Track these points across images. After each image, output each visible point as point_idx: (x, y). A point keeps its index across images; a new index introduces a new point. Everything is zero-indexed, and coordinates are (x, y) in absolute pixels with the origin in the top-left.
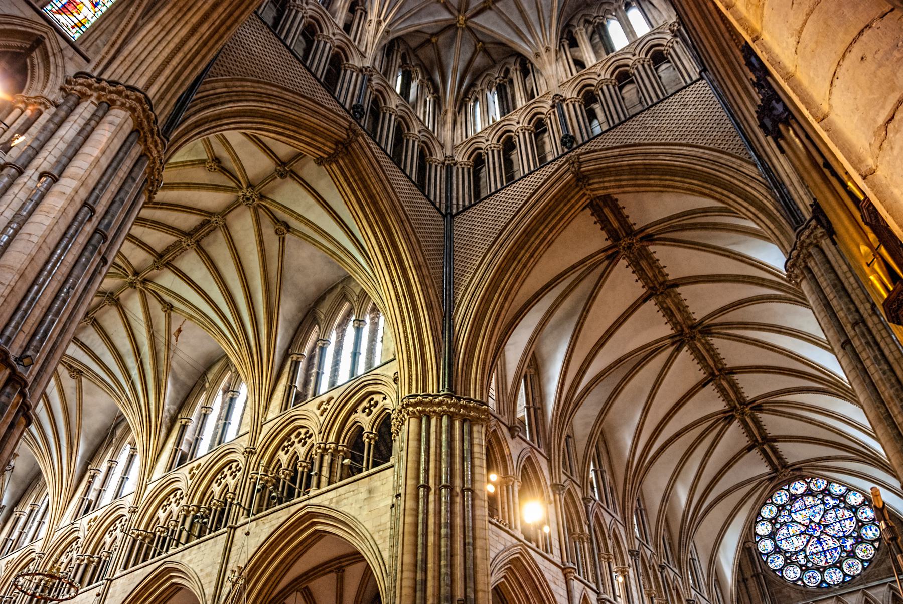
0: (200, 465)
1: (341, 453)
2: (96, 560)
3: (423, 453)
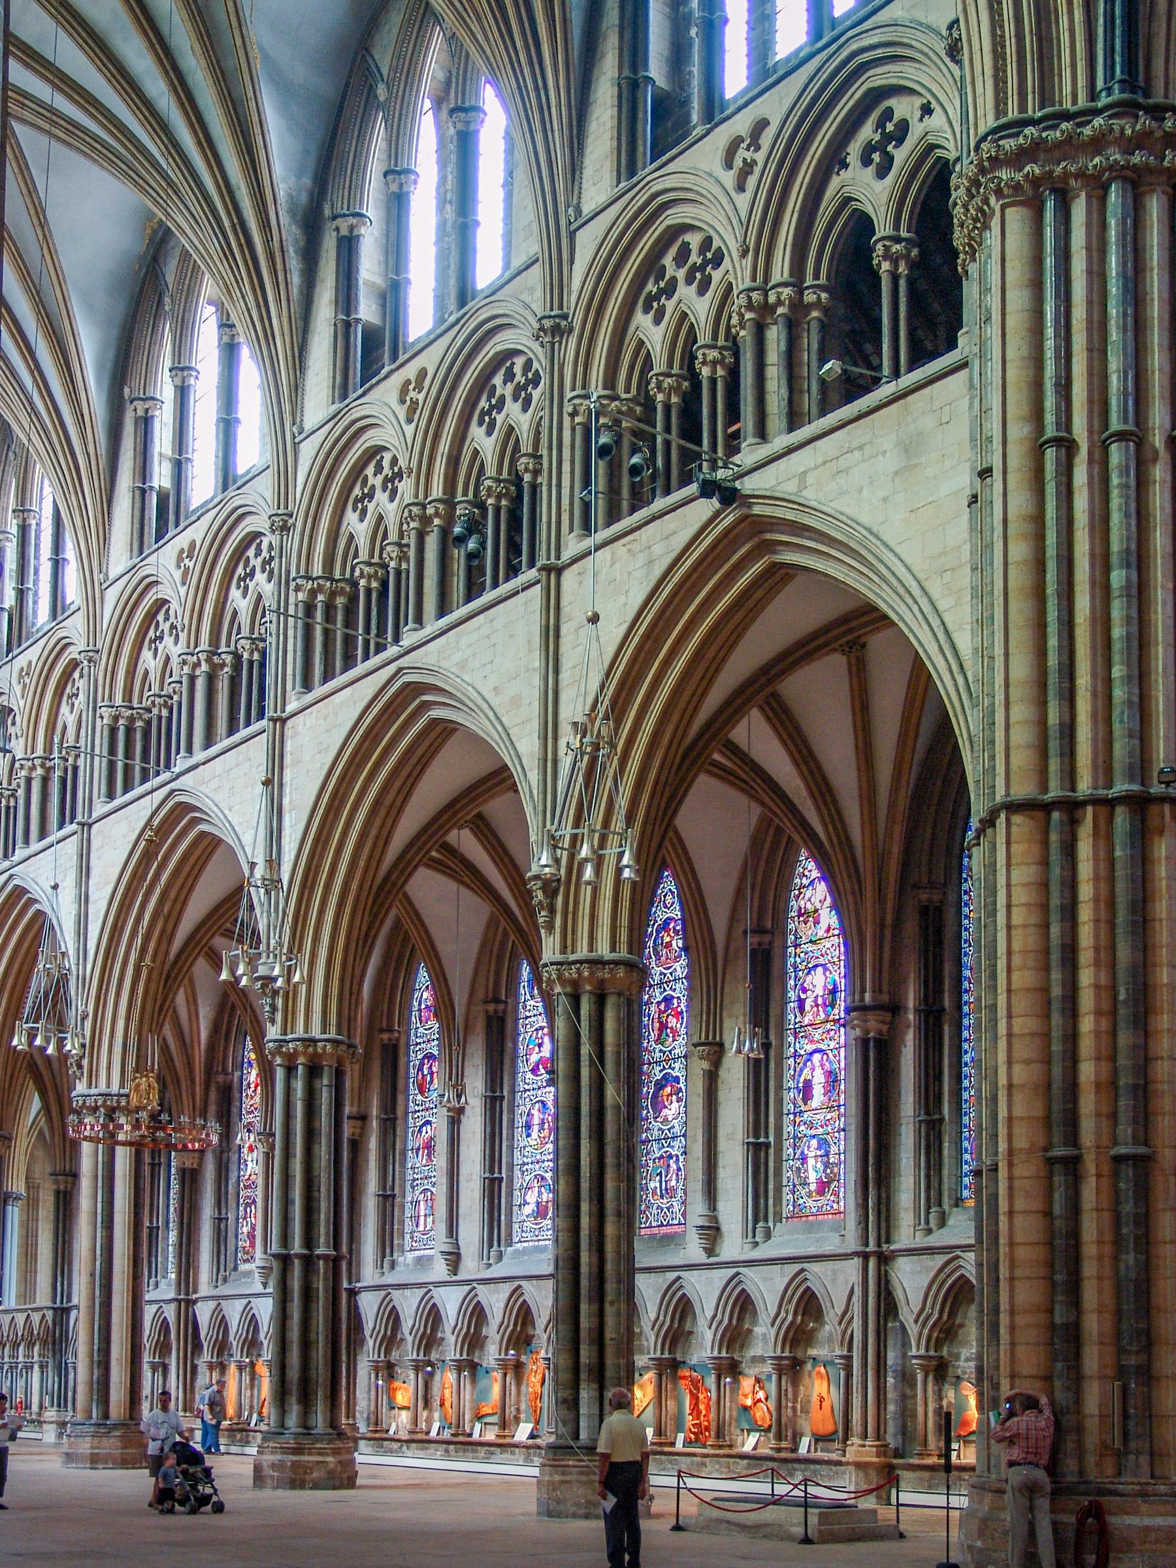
0: (423, 373)
1: (815, 314)
2: (228, 659)
3: (1050, 332)
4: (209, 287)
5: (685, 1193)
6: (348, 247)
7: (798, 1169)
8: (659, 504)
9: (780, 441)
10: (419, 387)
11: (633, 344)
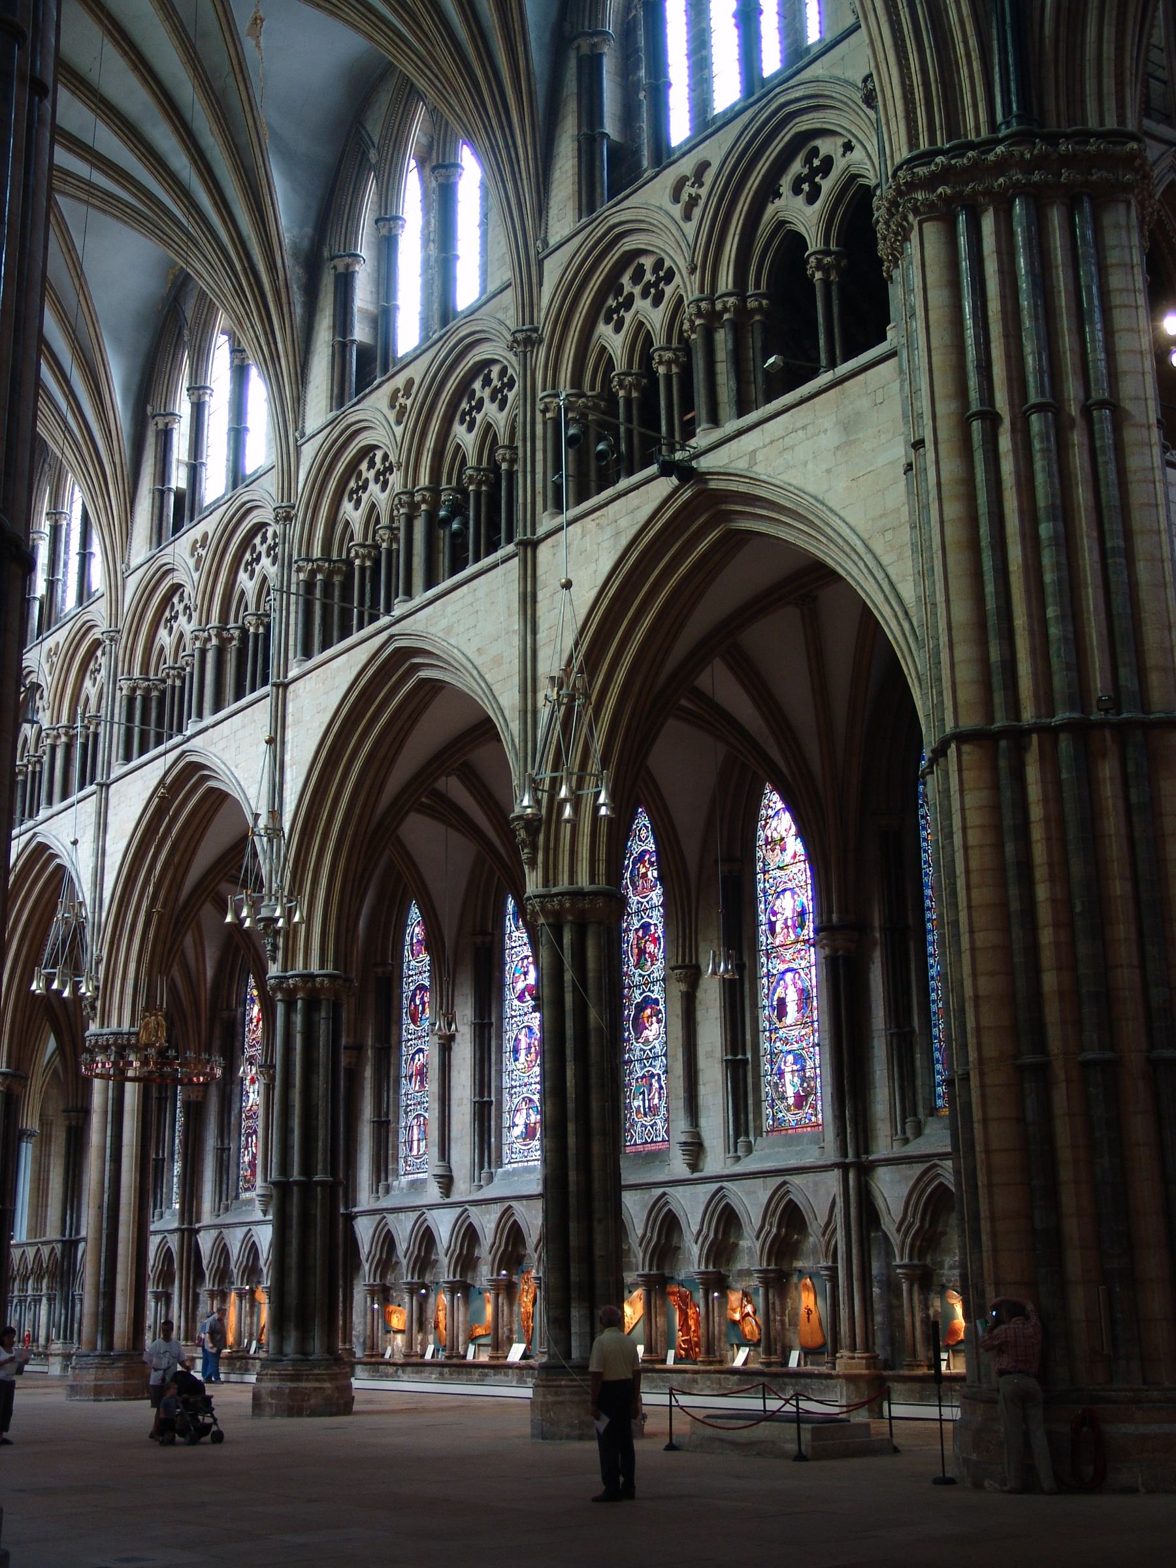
0: (410, 382)
1: (757, 318)
2: (236, 633)
4: (222, 320)
5: (668, 1110)
6: (345, 283)
7: (776, 1084)
8: (623, 484)
9: (731, 426)
10: (407, 394)
11: (597, 350)
